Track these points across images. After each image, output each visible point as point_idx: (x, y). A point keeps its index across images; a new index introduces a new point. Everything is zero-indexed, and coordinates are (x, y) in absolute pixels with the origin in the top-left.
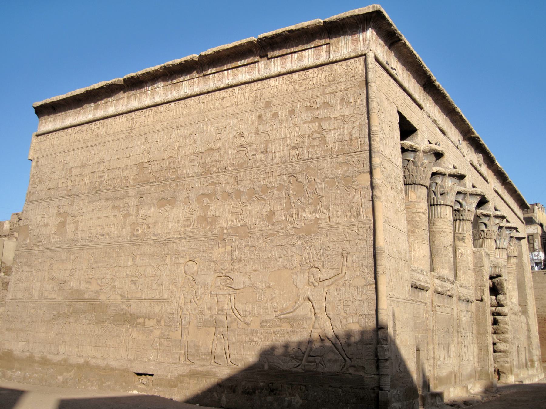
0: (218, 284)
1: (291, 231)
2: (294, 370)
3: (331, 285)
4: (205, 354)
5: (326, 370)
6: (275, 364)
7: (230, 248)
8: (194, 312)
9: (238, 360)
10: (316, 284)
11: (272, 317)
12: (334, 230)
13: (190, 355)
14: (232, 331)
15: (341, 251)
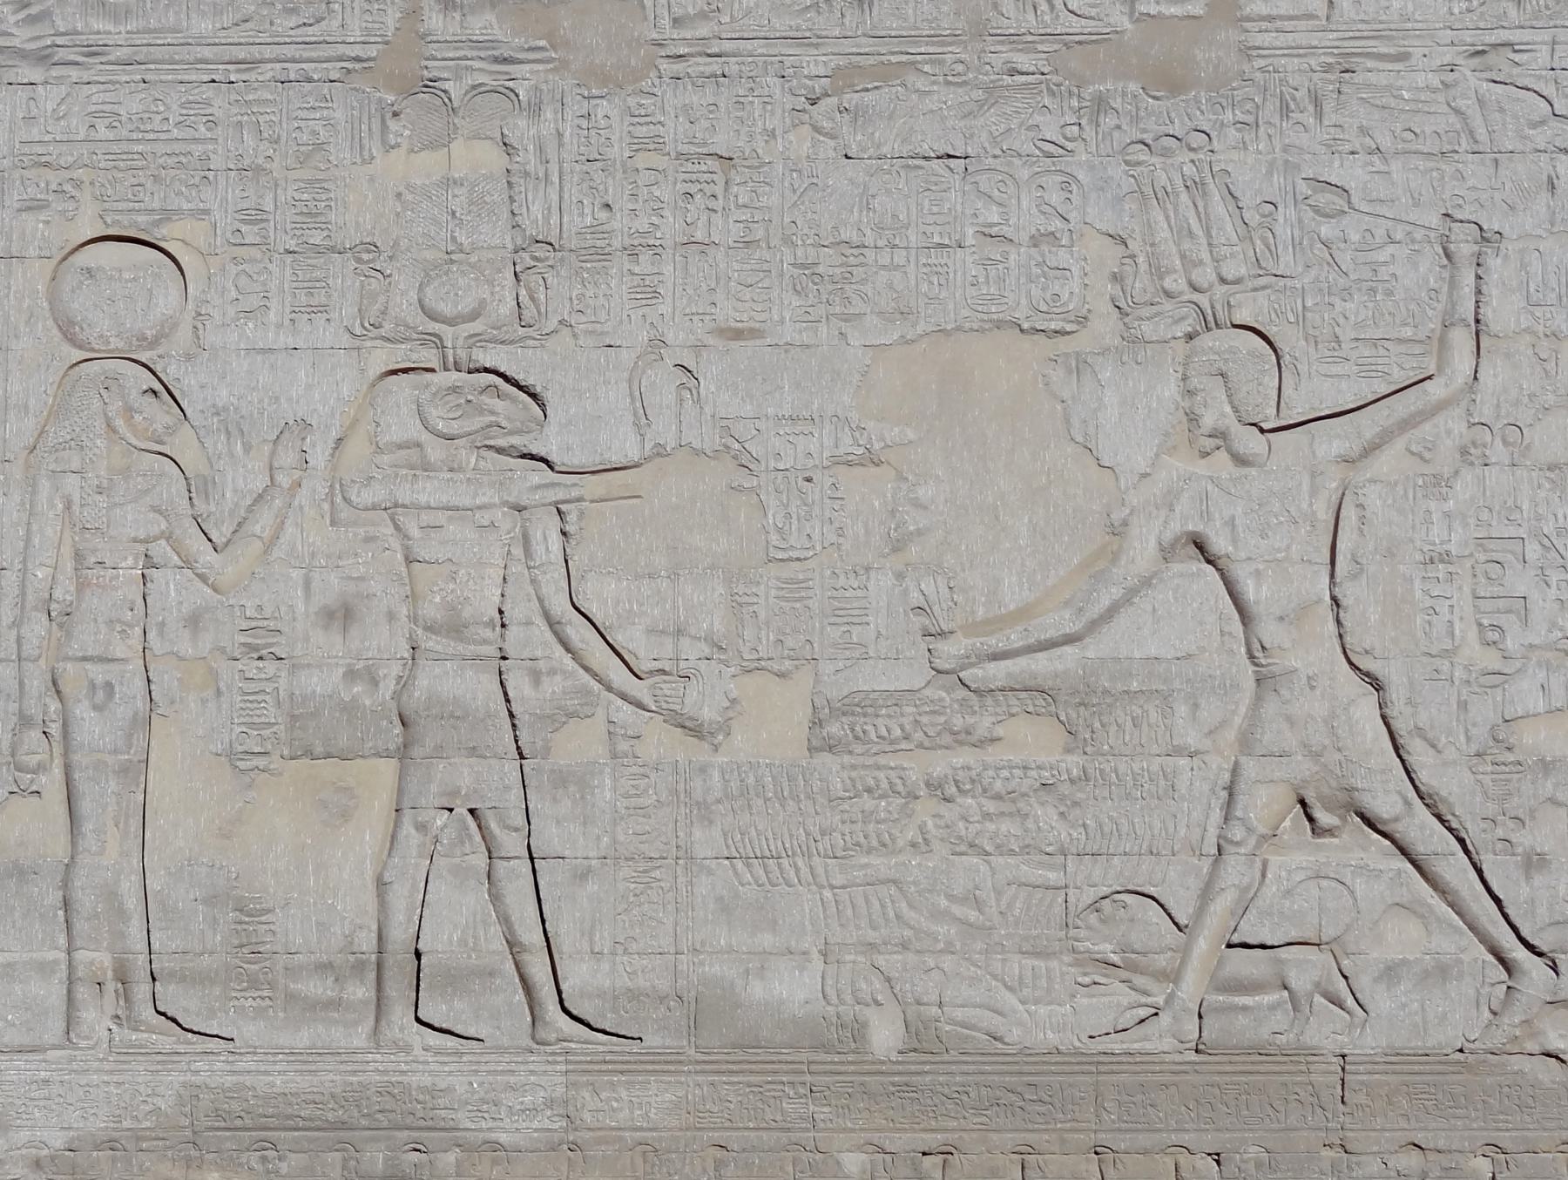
0: (400, 424)
1: (1023, 61)
2: (1116, 1044)
3: (1370, 450)
4: (324, 968)
5: (1370, 1042)
6: (959, 1014)
7: (493, 158)
8: (186, 648)
9: (634, 995)
10: (1253, 443)
11: (913, 676)
12: (1377, 75)
13: (182, 978)
14: (561, 780)
15: (1434, 220)
